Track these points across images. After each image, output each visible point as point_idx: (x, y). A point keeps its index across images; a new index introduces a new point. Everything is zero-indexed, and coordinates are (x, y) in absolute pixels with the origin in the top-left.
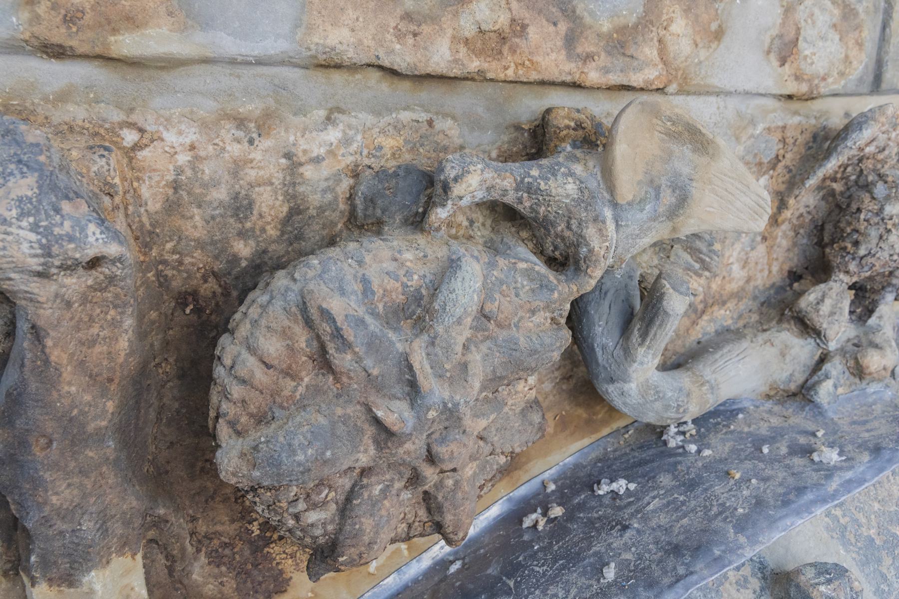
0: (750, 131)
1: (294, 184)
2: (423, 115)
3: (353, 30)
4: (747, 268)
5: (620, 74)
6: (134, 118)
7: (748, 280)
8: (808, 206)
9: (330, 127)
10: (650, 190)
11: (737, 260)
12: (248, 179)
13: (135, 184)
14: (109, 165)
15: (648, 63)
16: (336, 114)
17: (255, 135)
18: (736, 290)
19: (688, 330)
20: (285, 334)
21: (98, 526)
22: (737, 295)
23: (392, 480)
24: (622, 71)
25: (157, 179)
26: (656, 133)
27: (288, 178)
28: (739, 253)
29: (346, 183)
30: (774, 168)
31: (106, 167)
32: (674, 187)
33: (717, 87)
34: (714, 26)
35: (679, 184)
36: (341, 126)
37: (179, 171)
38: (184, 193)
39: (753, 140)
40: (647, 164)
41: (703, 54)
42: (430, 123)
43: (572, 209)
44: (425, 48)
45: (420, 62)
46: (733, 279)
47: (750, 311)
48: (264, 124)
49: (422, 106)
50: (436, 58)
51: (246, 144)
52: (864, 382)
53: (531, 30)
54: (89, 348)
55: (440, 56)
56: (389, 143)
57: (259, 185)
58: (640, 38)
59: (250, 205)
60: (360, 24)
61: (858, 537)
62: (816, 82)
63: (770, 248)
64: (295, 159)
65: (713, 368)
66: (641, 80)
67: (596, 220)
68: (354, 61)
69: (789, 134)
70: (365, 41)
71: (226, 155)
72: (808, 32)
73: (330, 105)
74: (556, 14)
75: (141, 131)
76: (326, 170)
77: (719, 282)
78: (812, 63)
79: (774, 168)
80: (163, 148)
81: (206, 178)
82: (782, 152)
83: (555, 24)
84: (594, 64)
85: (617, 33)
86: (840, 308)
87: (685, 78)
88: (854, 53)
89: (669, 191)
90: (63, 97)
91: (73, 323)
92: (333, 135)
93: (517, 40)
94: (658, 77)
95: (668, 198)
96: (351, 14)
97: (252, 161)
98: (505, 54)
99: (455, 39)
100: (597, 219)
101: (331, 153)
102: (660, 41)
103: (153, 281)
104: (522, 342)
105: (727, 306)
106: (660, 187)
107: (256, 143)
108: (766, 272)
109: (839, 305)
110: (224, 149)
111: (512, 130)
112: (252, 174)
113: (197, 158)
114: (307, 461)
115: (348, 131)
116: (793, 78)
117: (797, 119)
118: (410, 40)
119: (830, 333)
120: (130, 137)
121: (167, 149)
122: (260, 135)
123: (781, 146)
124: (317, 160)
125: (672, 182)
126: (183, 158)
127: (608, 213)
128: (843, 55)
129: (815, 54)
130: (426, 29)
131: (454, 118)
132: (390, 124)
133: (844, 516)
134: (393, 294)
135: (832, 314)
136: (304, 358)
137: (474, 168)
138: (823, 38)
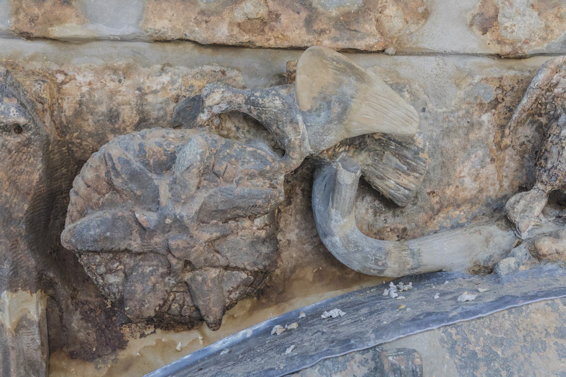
0: (469, 80)
1: (142, 105)
2: (218, 67)
3: (170, 21)
4: (478, 182)
5: (347, 42)
6: (63, 68)
7: (481, 191)
8: (526, 137)
9: (163, 74)
10: (324, 103)
11: (469, 174)
12: (117, 101)
13: (60, 101)
14: (41, 87)
15: (369, 35)
16: (167, 67)
17: (122, 78)
18: (469, 197)
19: (426, 223)
20: (97, 169)
21: (12, 268)
22: (472, 201)
23: (157, 266)
24: (348, 40)
25: (71, 99)
26: (331, 70)
27: (139, 101)
28: (470, 169)
29: (172, 105)
30: (495, 107)
31: (40, 89)
32: (340, 102)
33: (430, 50)
34: (421, 10)
35: (344, 100)
36: (170, 74)
37: (83, 95)
38: (84, 107)
39: (471, 86)
40: (322, 87)
41: (413, 28)
42: (223, 73)
43: (279, 115)
44: (213, 29)
45: (210, 37)
46: (466, 189)
47: (483, 215)
48: (127, 71)
49: (218, 63)
50: (219, 34)
51: (118, 83)
52: (542, 264)
53: (283, 18)
54: (18, 175)
55: (222, 33)
57: (123, 105)
58: (361, 20)
59: (118, 116)
60: (174, 17)
61: (464, 350)
62: (519, 44)
63: (499, 168)
64: (143, 91)
65: (422, 243)
66: (363, 45)
67: (291, 121)
68: (172, 37)
69: (505, 83)
70: (178, 26)
71: (107, 88)
73: (164, 62)
74: (298, 7)
75: (66, 74)
76: (160, 98)
77: (453, 190)
78: (513, 32)
79: (495, 107)
80: (75, 83)
81: (96, 99)
82: (500, 96)
83: (298, 13)
84: (326, 36)
85: (343, 16)
86: (531, 207)
87: (399, 44)
88: (554, 24)
89: (337, 105)
90: (33, 58)
91: (10, 160)
92: (165, 79)
93: (274, 23)
94: (376, 43)
95: (337, 109)
96: (170, 12)
97: (120, 91)
98: (267, 32)
100: (292, 121)
101: (164, 88)
102: (377, 20)
103: (65, 153)
105: (461, 209)
106: (331, 102)
107: (123, 82)
108: (498, 187)
109: (531, 205)
110: (106, 84)
111: (277, 77)
112: (120, 98)
113: (92, 89)
114: (95, 235)
115: (174, 77)
116: (495, 42)
117: (512, 73)
118: (204, 25)
119: (522, 226)
120: (60, 78)
121: (78, 84)
122: (124, 78)
123: (500, 92)
124: (155, 92)
125: (339, 99)
126: (85, 89)
127: (300, 118)
128: (543, 26)
129: (515, 25)
130: (213, 19)
131: (239, 70)
132: (197, 73)
133: (457, 334)
134: (158, 154)
135: (524, 211)
136: (104, 183)
137: (218, 90)
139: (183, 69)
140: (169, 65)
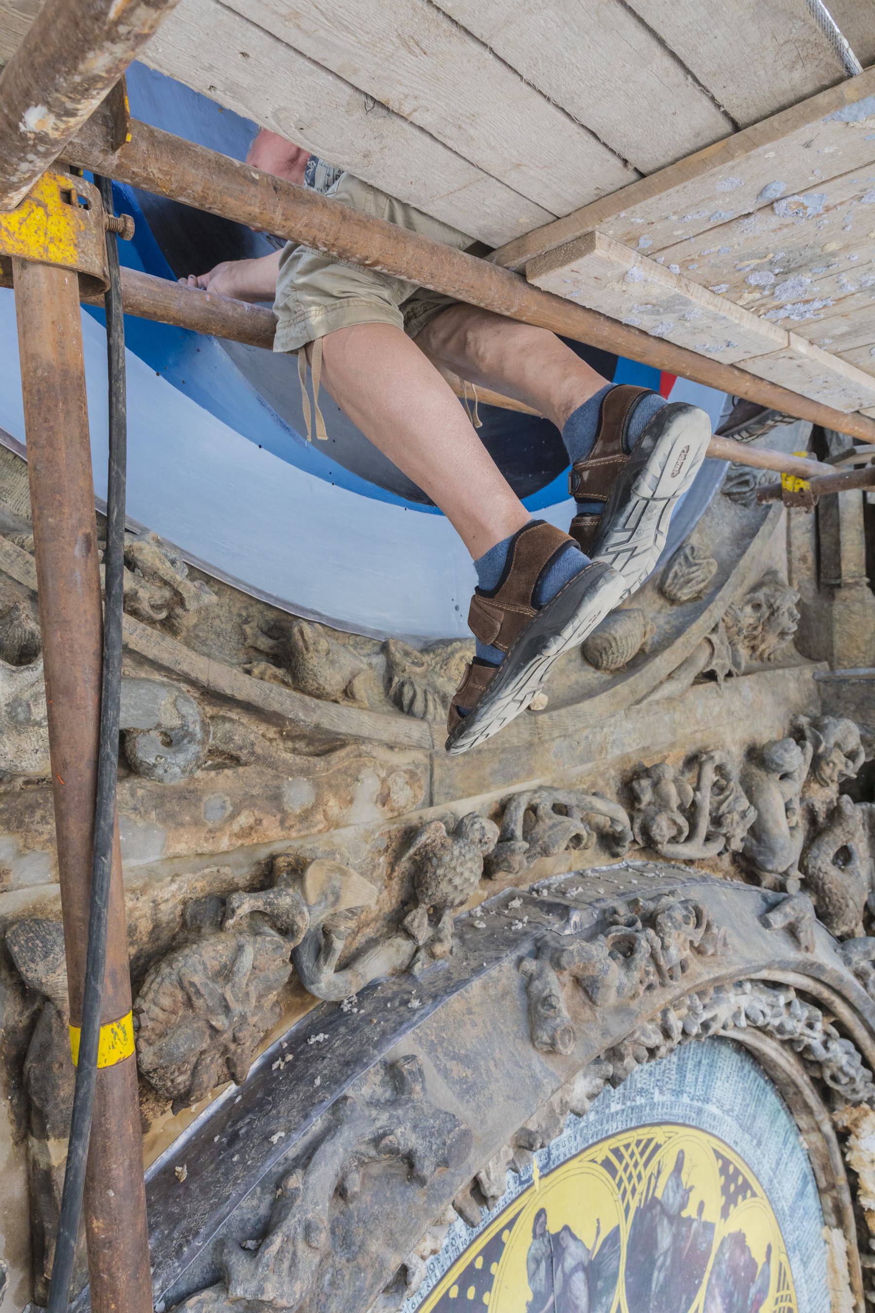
15: (320, 822)
20: (172, 995)
22: (375, 920)
29: (180, 907)
32: (333, 893)
41: (345, 811)
48: (143, 890)
53: (265, 822)
56: (199, 885)
61: (427, 1041)
69: (392, 834)
72: (395, 788)
76: (170, 904)
88: (418, 792)
92: (174, 887)
95: (331, 898)
96: (186, 836)
99: (230, 836)
100: (301, 913)
101: (173, 896)
104: (271, 977)
112: (137, 914)
117: (395, 826)
119: (419, 937)
124: (167, 901)
127: (305, 909)
130: (218, 834)
138: (402, 790)
139: (189, 876)
140: (177, 875)
